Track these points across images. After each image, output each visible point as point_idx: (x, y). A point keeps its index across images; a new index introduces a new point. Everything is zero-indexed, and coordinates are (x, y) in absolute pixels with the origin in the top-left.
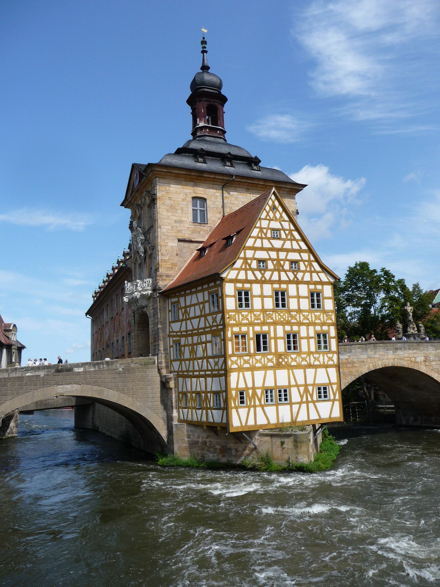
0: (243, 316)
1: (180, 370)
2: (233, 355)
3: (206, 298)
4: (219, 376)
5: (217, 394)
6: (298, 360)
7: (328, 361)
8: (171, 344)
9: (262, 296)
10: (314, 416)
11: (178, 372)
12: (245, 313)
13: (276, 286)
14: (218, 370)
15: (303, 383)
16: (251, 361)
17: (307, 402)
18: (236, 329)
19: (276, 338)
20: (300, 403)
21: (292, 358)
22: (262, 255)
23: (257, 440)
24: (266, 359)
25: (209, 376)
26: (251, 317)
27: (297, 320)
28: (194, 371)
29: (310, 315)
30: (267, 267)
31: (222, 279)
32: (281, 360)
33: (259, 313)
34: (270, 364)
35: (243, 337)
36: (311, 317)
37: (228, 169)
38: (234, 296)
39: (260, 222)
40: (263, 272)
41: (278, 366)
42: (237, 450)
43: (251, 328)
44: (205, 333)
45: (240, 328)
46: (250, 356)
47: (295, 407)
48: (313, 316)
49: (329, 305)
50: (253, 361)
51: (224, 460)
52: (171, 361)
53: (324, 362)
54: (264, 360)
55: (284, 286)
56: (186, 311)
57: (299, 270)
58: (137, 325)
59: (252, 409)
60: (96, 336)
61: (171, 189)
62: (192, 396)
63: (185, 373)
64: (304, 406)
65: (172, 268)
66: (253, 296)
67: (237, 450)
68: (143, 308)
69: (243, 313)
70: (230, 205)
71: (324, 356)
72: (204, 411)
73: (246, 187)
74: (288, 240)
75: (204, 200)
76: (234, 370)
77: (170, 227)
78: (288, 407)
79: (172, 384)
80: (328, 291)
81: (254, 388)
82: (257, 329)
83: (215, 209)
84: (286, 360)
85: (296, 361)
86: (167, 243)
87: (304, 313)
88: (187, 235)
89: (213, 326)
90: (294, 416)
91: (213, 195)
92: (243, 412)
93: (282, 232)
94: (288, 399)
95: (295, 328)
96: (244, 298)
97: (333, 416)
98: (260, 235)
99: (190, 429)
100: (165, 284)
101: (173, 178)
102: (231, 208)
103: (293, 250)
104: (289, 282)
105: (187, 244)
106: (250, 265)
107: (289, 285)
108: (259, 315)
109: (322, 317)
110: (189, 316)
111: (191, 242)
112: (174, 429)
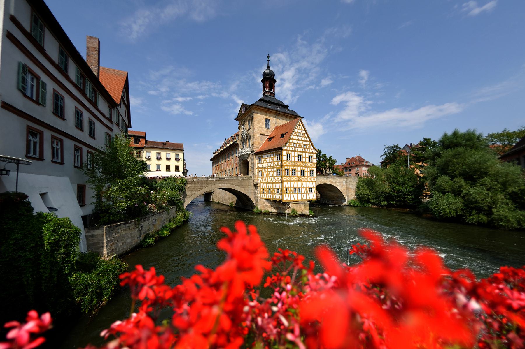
5: (278, 189)
9: (294, 156)
10: (308, 198)
18: (286, 167)
19: (298, 171)
22: (295, 142)
23: (290, 205)
26: (291, 164)
31: (282, 149)
35: (288, 170)
36: (309, 165)
37: (278, 109)
41: (298, 181)
44: (273, 168)
47: (303, 195)
49: (315, 161)
60: (215, 168)
75: (269, 120)
76: (284, 181)
79: (258, 185)
80: (315, 156)
81: (291, 188)
82: (292, 167)
88: (263, 133)
91: (273, 120)
92: (287, 195)
96: (288, 156)
100: (256, 150)
103: (305, 141)
104: (303, 152)
111: (265, 135)
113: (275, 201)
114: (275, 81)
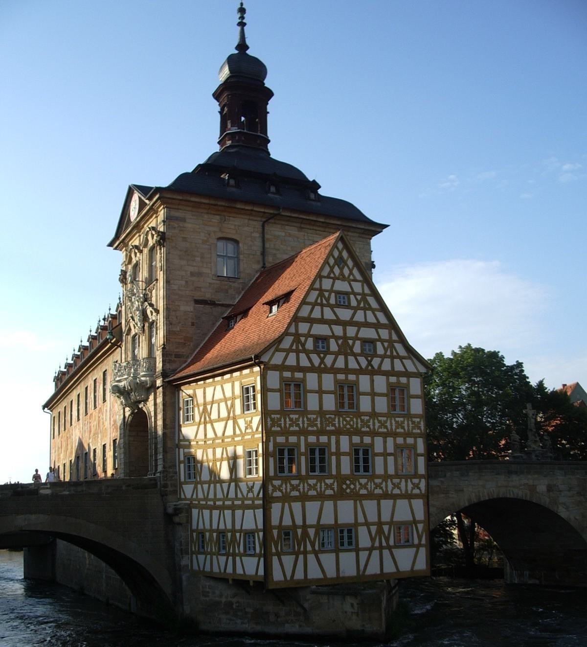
0: (291, 420)
1: (194, 496)
2: (276, 477)
3: (238, 391)
4: (253, 507)
5: (250, 534)
6: (369, 487)
7: (413, 489)
8: (182, 458)
9: (320, 392)
10: (389, 568)
11: (191, 499)
12: (294, 417)
13: (341, 377)
14: (253, 499)
15: (376, 520)
16: (301, 487)
17: (381, 548)
18: (281, 439)
19: (338, 454)
20: (371, 550)
21: (360, 484)
22: (321, 330)
24: (323, 484)
25: (239, 507)
26: (303, 423)
27: (370, 428)
28: (215, 499)
29: (389, 422)
30: (328, 348)
32: (344, 487)
33: (315, 416)
34: (329, 492)
36: (391, 424)
38: (280, 390)
39: (321, 281)
40: (322, 355)
41: (340, 495)
42: (277, 615)
43: (302, 438)
45: (287, 439)
46: (299, 479)
48: (393, 422)
49: (417, 407)
50: (304, 486)
51: (258, 628)
52: (181, 484)
53: (406, 490)
54: (321, 486)
55: (352, 377)
56: (205, 409)
57: (375, 355)
58: (128, 428)
59: (301, 557)
61: (186, 225)
62: (211, 536)
63: (201, 502)
64: (376, 553)
65: (185, 343)
66: (307, 391)
67: (277, 615)
68: (140, 402)
69: (291, 416)
70: (274, 252)
71: (406, 482)
72: (230, 558)
73: (298, 225)
74: (361, 309)
75: (236, 242)
76: (277, 499)
77: (183, 283)
78: (354, 554)
80: (415, 386)
81: (305, 527)
82: (312, 439)
83: (251, 257)
84: (352, 486)
85: (366, 488)
86: (179, 306)
87: (380, 418)
88: (208, 296)
89: (246, 434)
90: (362, 568)
92: (288, 560)
93: (352, 297)
94: (354, 543)
95: (367, 440)
97: (416, 568)
98: (319, 301)
99: (208, 584)
101: (190, 209)
102: (275, 255)
103: (367, 324)
104: (360, 371)
105: (208, 308)
106: (303, 345)
107: (360, 376)
108: (316, 420)
109: (405, 425)
110: (210, 418)
112: (185, 583)
113: (242, 584)
114: (269, 94)
